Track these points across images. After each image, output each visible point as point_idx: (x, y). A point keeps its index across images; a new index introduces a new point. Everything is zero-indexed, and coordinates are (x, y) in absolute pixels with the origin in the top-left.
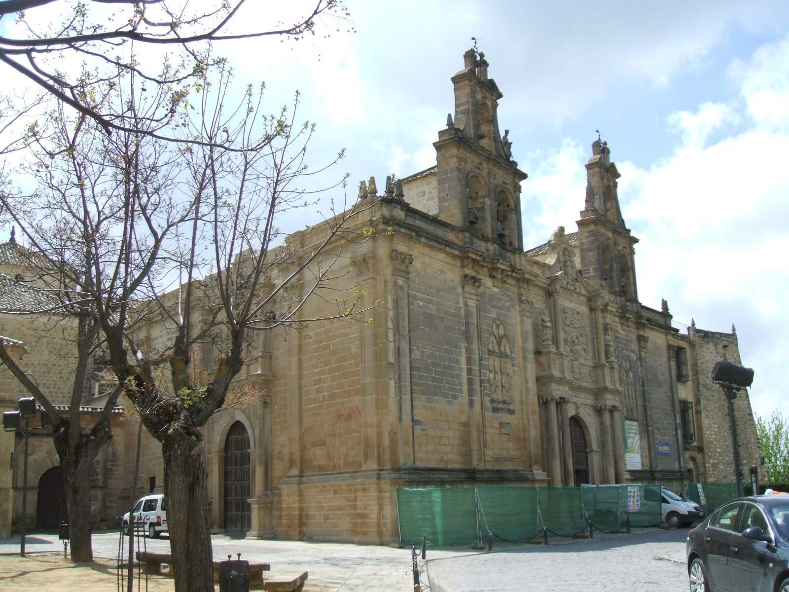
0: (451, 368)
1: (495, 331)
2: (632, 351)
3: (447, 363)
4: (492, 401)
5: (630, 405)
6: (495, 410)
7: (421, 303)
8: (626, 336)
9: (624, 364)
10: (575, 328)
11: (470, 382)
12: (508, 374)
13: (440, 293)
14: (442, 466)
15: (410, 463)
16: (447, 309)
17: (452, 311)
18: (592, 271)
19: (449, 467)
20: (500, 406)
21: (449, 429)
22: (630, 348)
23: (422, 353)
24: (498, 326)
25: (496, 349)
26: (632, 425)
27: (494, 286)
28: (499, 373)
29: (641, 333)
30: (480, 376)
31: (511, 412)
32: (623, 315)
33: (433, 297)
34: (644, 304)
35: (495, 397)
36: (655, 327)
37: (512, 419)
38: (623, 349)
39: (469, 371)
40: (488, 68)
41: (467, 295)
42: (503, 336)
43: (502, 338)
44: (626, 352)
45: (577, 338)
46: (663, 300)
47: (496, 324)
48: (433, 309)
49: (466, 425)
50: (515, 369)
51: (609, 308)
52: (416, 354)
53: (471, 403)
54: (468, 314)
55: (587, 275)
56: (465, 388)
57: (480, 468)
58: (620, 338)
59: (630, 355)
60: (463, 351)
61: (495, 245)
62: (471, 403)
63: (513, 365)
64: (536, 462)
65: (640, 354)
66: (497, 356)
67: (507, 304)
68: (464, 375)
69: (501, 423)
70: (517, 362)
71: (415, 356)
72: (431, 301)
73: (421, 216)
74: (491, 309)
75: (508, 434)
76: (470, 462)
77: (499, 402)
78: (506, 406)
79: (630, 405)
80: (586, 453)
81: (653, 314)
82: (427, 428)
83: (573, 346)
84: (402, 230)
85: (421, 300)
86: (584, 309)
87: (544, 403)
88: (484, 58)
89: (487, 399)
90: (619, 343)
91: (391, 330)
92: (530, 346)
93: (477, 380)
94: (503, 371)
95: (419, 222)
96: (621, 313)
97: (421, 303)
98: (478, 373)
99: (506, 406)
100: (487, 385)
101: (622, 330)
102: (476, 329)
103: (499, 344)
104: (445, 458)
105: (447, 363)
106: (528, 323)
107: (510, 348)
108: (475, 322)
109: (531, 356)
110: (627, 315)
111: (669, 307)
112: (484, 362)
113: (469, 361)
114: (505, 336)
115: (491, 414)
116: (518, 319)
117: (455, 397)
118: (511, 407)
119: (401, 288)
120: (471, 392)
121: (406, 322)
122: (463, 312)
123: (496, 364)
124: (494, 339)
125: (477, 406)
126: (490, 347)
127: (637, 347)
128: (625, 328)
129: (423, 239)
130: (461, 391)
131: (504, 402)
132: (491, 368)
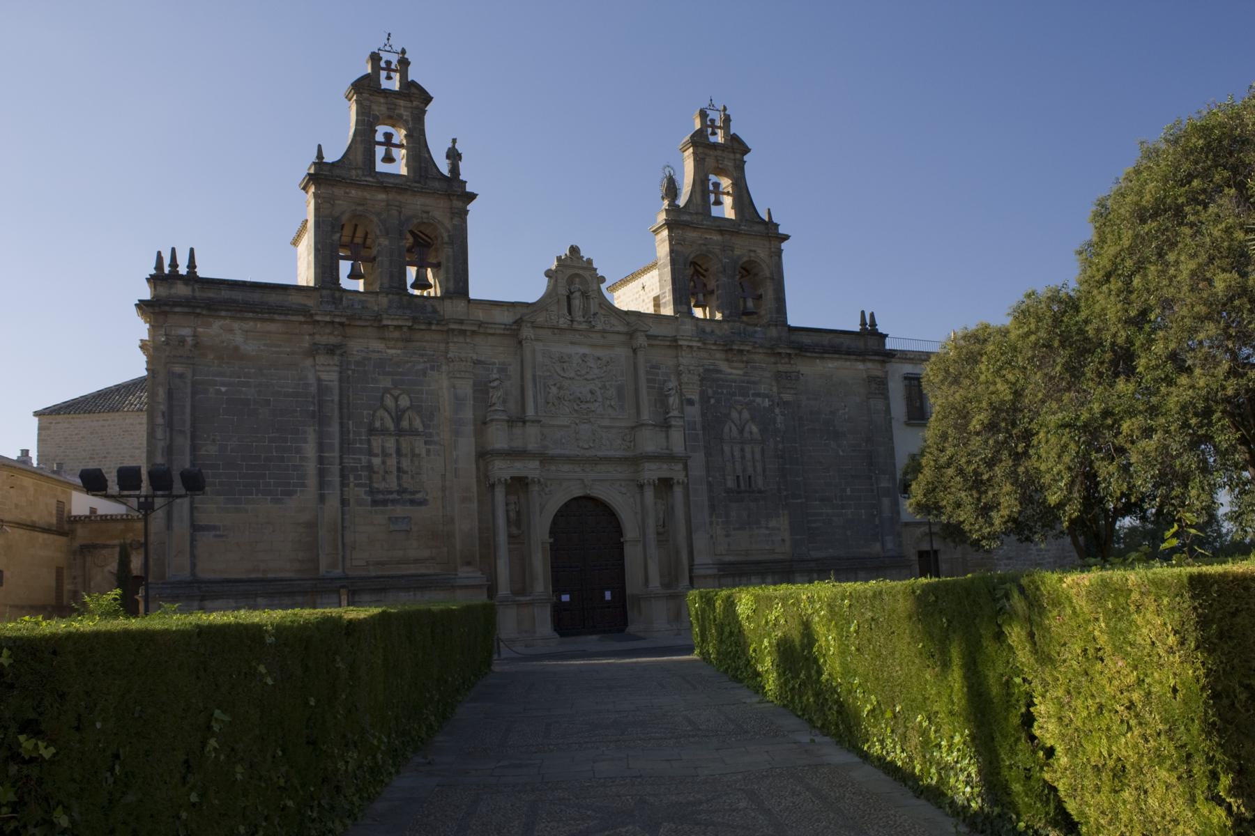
1: (389, 401)
2: (758, 395)
3: (275, 454)
4: (372, 492)
5: (744, 470)
6: (375, 503)
7: (223, 389)
8: (745, 374)
9: (735, 415)
10: (586, 379)
11: (322, 473)
12: (419, 455)
14: (253, 576)
15: (185, 574)
16: (279, 389)
18: (667, 294)
19: (271, 576)
20: (395, 496)
22: (753, 391)
24: (396, 399)
25: (390, 425)
27: (388, 348)
28: (394, 455)
29: (781, 368)
30: (341, 463)
31: (423, 503)
32: (728, 347)
34: (792, 325)
35: (382, 486)
36: (826, 355)
39: (321, 460)
40: (410, 68)
41: (317, 368)
42: (408, 408)
43: (404, 411)
45: (592, 392)
46: (863, 313)
47: (392, 395)
49: (312, 526)
50: (432, 447)
51: (680, 343)
53: (322, 498)
54: (323, 389)
55: (664, 301)
56: (312, 481)
59: (754, 401)
60: (311, 436)
61: (390, 296)
62: (322, 498)
63: (426, 443)
64: (469, 564)
65: (781, 398)
66: (390, 434)
67: (420, 367)
68: (311, 468)
70: (436, 439)
71: (207, 451)
73: (228, 284)
75: (407, 531)
76: (318, 569)
77: (391, 493)
78: (407, 496)
79: (744, 470)
80: (622, 543)
81: (831, 336)
83: (578, 405)
84: (178, 309)
85: (223, 384)
86: (622, 353)
87: (487, 485)
88: (406, 56)
89: (361, 492)
91: (161, 427)
92: (468, 414)
93: (336, 469)
94: (404, 451)
96: (725, 345)
97: (223, 389)
98: (337, 461)
99: (407, 496)
100: (364, 473)
101: (732, 368)
102: (336, 407)
103: (398, 419)
105: (275, 454)
106: (466, 388)
107: (423, 422)
108: (336, 398)
109: (470, 429)
110: (735, 347)
111: (877, 322)
112: (358, 445)
113: (321, 447)
114: (411, 407)
115: (369, 508)
116: (445, 383)
117: (290, 494)
118: (419, 496)
119: (181, 376)
120: (322, 484)
121: (188, 417)
122: (313, 389)
123: (388, 445)
125: (333, 502)
126: (378, 424)
127: (775, 389)
128: (735, 364)
129: (223, 313)
130: (303, 485)
131: (402, 491)
132: (377, 450)
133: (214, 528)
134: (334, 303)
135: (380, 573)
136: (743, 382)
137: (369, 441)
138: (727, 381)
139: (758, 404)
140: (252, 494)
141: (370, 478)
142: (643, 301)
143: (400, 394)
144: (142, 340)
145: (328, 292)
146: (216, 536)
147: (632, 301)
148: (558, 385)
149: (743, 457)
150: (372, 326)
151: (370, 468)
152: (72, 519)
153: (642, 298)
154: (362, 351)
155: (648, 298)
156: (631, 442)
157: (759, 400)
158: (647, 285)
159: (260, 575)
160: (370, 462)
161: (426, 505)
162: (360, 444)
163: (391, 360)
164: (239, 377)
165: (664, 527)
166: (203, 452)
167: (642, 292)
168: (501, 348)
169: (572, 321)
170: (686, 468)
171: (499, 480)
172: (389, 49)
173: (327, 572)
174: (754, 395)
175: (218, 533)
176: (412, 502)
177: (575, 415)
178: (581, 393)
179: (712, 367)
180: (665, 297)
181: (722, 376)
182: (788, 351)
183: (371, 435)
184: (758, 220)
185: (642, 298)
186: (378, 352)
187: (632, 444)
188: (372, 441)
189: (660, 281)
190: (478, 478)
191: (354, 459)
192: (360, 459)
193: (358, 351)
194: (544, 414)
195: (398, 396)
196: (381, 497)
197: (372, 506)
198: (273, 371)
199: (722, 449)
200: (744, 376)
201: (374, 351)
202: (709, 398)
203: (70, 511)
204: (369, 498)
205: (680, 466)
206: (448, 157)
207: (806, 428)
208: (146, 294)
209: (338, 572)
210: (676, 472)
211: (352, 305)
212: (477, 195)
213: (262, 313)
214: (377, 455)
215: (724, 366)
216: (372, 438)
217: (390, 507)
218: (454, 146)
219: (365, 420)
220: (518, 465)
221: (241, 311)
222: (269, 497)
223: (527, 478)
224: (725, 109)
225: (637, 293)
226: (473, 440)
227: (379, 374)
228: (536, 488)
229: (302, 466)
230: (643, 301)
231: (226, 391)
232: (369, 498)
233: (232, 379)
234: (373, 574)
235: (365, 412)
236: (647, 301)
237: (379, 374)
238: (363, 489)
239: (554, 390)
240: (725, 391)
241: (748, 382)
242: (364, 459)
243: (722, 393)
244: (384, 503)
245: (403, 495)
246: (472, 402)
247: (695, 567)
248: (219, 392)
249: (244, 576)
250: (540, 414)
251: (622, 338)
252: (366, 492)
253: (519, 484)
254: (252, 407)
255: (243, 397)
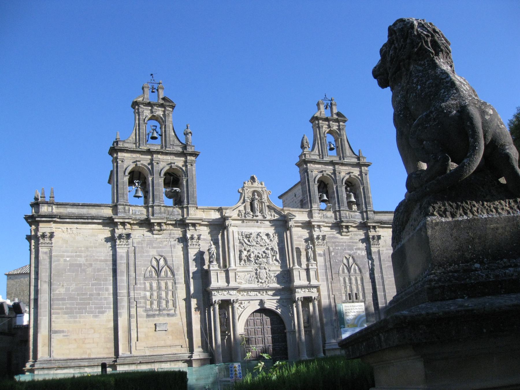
0: (99, 294)
4: (146, 310)
5: (351, 290)
6: (148, 316)
7: (68, 259)
8: (351, 238)
13: (90, 249)
14: (83, 357)
15: (47, 357)
16: (97, 258)
17: (103, 258)
21: (94, 332)
22: (355, 247)
23: (68, 289)
26: (354, 306)
33: (82, 253)
37: (173, 320)
38: (345, 249)
44: (349, 252)
45: (264, 252)
48: (82, 260)
51: (313, 223)
52: (59, 290)
57: (125, 356)
58: (338, 242)
59: (356, 252)
69: (155, 325)
71: (59, 291)
72: (80, 256)
74: (151, 250)
75: (166, 331)
80: (286, 333)
82: (69, 334)
85: (68, 257)
90: (336, 246)
95: (70, 209)
97: (68, 259)
100: (142, 301)
104: (88, 351)
105: (94, 292)
112: (139, 286)
115: (145, 319)
117: (103, 312)
124: (153, 270)
133: (63, 332)
134: (125, 212)
135: (151, 354)
136: (350, 242)
137: (145, 283)
138: (340, 243)
139: (359, 254)
140: (83, 314)
141: (146, 303)
142: (296, 202)
143: (161, 258)
144: (27, 236)
145: (122, 206)
146: (64, 336)
147: (291, 202)
148: (247, 249)
149: (351, 283)
150: (145, 223)
151: (145, 297)
152: (16, 327)
153: (295, 201)
154: (140, 236)
155: (298, 200)
156: (288, 278)
157: (359, 252)
158: (297, 193)
159: (87, 357)
160: (145, 294)
161: (176, 316)
162: (140, 285)
163: (156, 240)
164: (76, 252)
165: (308, 323)
166: (57, 292)
167: (295, 198)
168: (215, 232)
169: (253, 215)
170: (318, 291)
171: (215, 302)
172: (153, 82)
173: (122, 354)
174: (356, 249)
175: (65, 334)
176: (168, 315)
177: (256, 265)
178: (258, 253)
179: (332, 236)
180: (305, 200)
181: (338, 240)
182: (374, 224)
183: (146, 280)
184: (354, 156)
185: (295, 201)
186: (149, 236)
187: (289, 279)
188: (147, 283)
189: (302, 191)
190: (203, 300)
191: (136, 293)
192: (140, 293)
193: (138, 237)
194: (239, 265)
195: (159, 260)
196: (151, 313)
197: (147, 318)
198: (94, 248)
199: (339, 280)
200: (350, 239)
201: (147, 236)
202: (332, 252)
203: (15, 323)
204: (145, 314)
205: (315, 290)
206: (184, 134)
207: (387, 265)
208: (30, 212)
209: (128, 354)
210: (314, 294)
211: (135, 213)
212: (199, 153)
213: (87, 219)
214: (148, 291)
215: (338, 235)
216: (146, 282)
217: (156, 318)
218: (187, 128)
219: (143, 272)
220: (225, 293)
221: (76, 219)
222: (92, 315)
223: (230, 300)
224: (332, 100)
225: (293, 198)
226: (200, 281)
227: (150, 248)
228: (236, 305)
229: (110, 298)
230: (296, 202)
231: (69, 260)
232: (145, 314)
233: (72, 254)
234: (148, 354)
235: (142, 268)
236: (297, 202)
237: (150, 248)
238: (142, 309)
239: (245, 253)
240: (340, 248)
241: (352, 243)
242: (142, 293)
243: (339, 249)
244: (154, 316)
245: (163, 311)
246: (200, 261)
247: (326, 345)
248: (65, 261)
249: (79, 357)
250: (236, 265)
251: (281, 223)
252: (143, 311)
253: (225, 304)
254: (82, 268)
255: (78, 263)
